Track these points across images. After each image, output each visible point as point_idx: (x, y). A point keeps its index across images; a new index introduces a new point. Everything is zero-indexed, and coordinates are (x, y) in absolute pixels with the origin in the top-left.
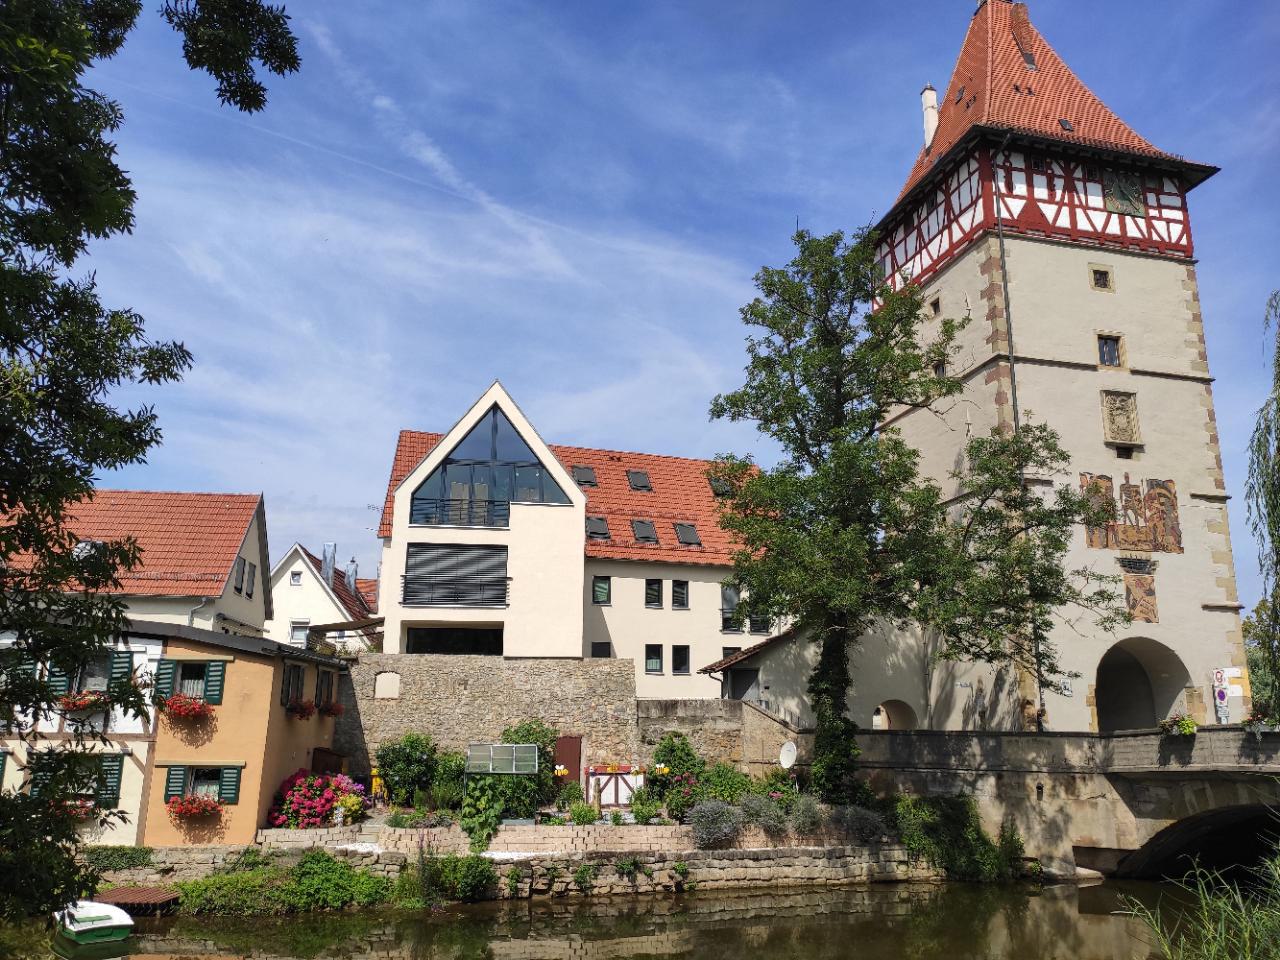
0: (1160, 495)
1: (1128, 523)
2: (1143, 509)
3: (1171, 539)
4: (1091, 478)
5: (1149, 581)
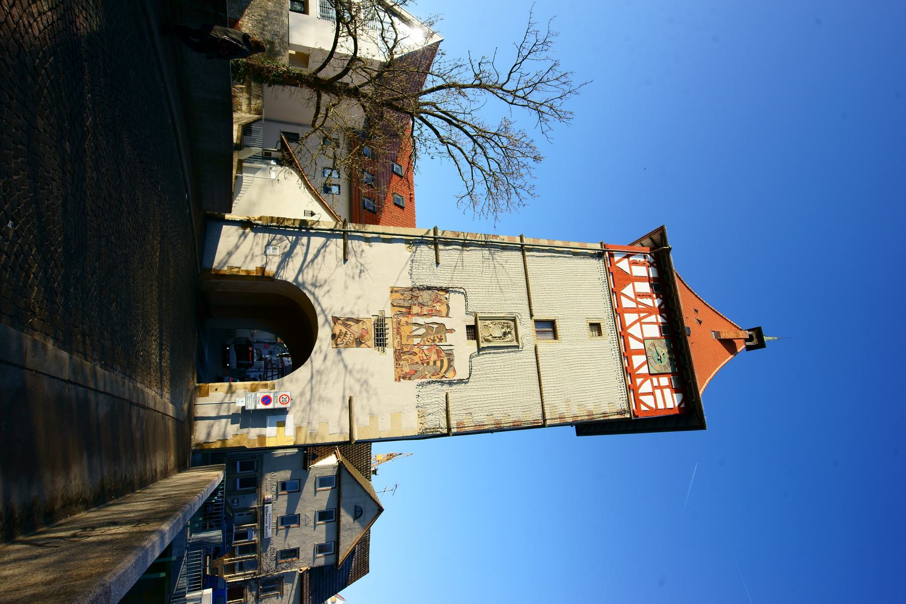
0: (442, 361)
1: (415, 328)
2: (427, 343)
3: (407, 369)
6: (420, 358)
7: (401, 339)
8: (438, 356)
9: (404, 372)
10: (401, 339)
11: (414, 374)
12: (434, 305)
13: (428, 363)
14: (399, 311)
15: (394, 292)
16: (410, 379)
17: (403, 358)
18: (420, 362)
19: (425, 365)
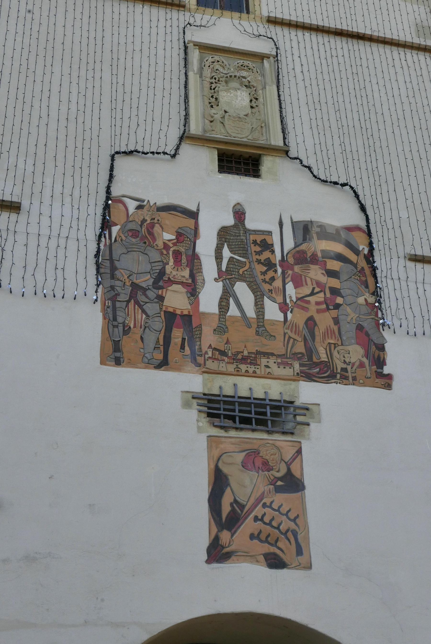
0: (327, 255)
1: (233, 311)
2: (278, 283)
4: (140, 207)
5: (289, 454)
6: (323, 311)
7: (267, 355)
8: (314, 260)
9: (365, 360)
10: (267, 355)
11: (367, 334)
12: (161, 245)
13: (335, 292)
14: (183, 347)
15: (118, 354)
16: (381, 348)
17: (324, 357)
18: (334, 313)
19: (339, 300)
